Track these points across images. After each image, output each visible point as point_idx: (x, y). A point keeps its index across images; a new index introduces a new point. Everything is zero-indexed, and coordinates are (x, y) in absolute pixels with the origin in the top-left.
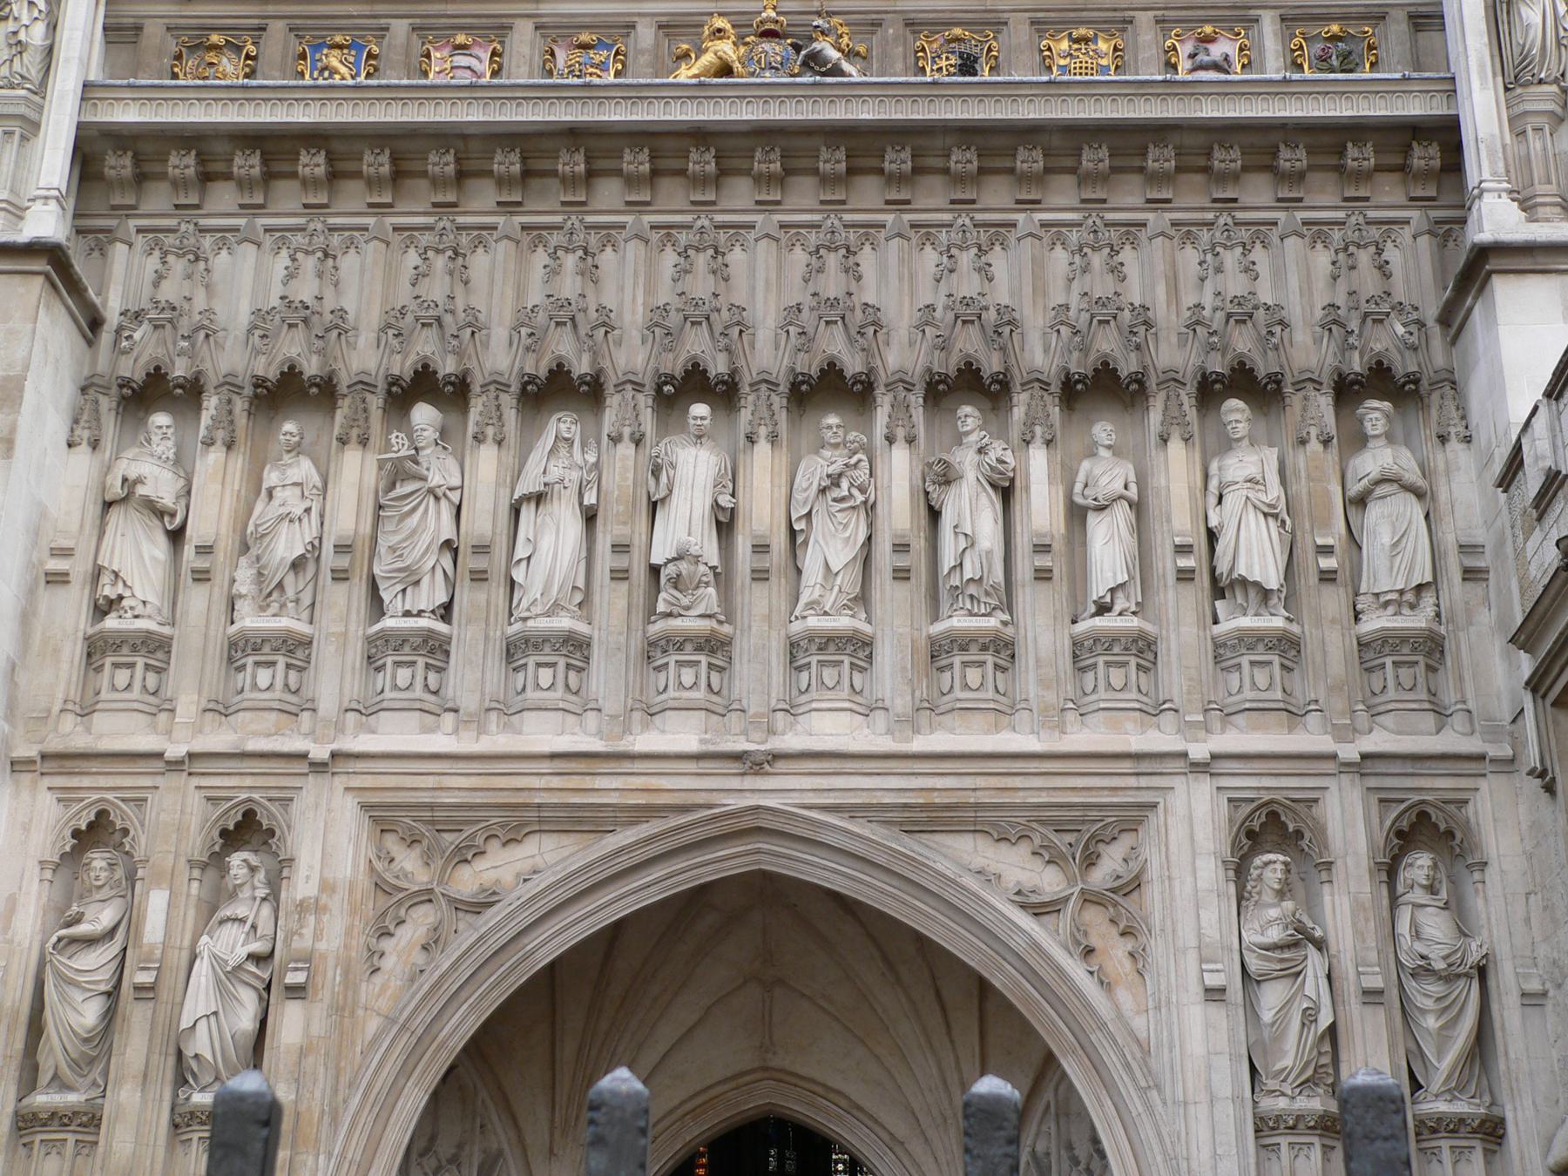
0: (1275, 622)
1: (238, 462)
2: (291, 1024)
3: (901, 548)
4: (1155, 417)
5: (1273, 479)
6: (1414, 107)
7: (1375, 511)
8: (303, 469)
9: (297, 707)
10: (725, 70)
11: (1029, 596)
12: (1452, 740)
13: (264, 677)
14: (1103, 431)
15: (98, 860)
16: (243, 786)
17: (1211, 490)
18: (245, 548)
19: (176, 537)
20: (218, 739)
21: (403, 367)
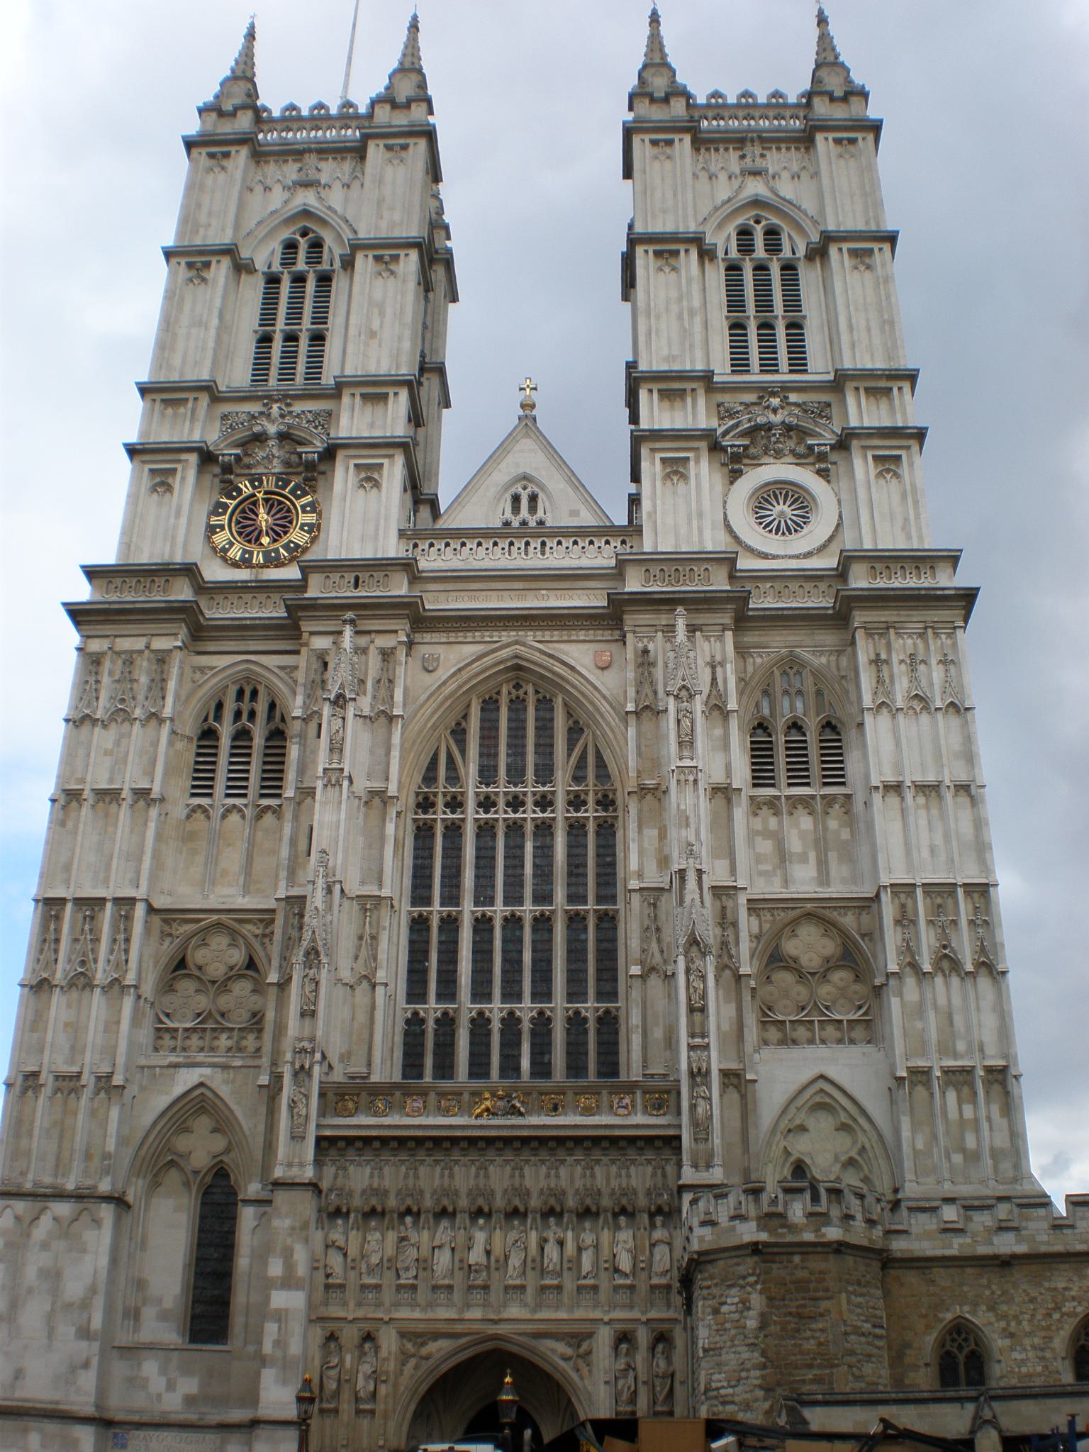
0: (628, 1282)
1: (360, 1234)
2: (383, 1390)
3: (533, 1261)
4: (601, 1221)
5: (631, 1240)
6: (671, 1132)
7: (657, 1250)
8: (378, 1235)
9: (379, 1305)
10: (487, 1110)
11: (566, 1273)
12: (671, 1314)
13: (370, 1296)
14: (587, 1225)
15: (333, 1345)
16: (367, 1326)
17: (614, 1242)
18: (363, 1257)
19: (345, 1255)
20: (360, 1313)
21: (403, 1208)
